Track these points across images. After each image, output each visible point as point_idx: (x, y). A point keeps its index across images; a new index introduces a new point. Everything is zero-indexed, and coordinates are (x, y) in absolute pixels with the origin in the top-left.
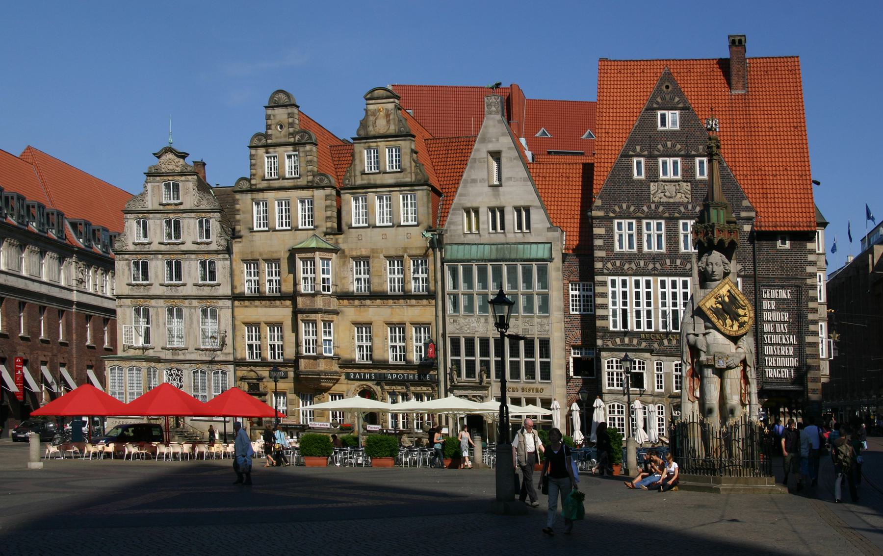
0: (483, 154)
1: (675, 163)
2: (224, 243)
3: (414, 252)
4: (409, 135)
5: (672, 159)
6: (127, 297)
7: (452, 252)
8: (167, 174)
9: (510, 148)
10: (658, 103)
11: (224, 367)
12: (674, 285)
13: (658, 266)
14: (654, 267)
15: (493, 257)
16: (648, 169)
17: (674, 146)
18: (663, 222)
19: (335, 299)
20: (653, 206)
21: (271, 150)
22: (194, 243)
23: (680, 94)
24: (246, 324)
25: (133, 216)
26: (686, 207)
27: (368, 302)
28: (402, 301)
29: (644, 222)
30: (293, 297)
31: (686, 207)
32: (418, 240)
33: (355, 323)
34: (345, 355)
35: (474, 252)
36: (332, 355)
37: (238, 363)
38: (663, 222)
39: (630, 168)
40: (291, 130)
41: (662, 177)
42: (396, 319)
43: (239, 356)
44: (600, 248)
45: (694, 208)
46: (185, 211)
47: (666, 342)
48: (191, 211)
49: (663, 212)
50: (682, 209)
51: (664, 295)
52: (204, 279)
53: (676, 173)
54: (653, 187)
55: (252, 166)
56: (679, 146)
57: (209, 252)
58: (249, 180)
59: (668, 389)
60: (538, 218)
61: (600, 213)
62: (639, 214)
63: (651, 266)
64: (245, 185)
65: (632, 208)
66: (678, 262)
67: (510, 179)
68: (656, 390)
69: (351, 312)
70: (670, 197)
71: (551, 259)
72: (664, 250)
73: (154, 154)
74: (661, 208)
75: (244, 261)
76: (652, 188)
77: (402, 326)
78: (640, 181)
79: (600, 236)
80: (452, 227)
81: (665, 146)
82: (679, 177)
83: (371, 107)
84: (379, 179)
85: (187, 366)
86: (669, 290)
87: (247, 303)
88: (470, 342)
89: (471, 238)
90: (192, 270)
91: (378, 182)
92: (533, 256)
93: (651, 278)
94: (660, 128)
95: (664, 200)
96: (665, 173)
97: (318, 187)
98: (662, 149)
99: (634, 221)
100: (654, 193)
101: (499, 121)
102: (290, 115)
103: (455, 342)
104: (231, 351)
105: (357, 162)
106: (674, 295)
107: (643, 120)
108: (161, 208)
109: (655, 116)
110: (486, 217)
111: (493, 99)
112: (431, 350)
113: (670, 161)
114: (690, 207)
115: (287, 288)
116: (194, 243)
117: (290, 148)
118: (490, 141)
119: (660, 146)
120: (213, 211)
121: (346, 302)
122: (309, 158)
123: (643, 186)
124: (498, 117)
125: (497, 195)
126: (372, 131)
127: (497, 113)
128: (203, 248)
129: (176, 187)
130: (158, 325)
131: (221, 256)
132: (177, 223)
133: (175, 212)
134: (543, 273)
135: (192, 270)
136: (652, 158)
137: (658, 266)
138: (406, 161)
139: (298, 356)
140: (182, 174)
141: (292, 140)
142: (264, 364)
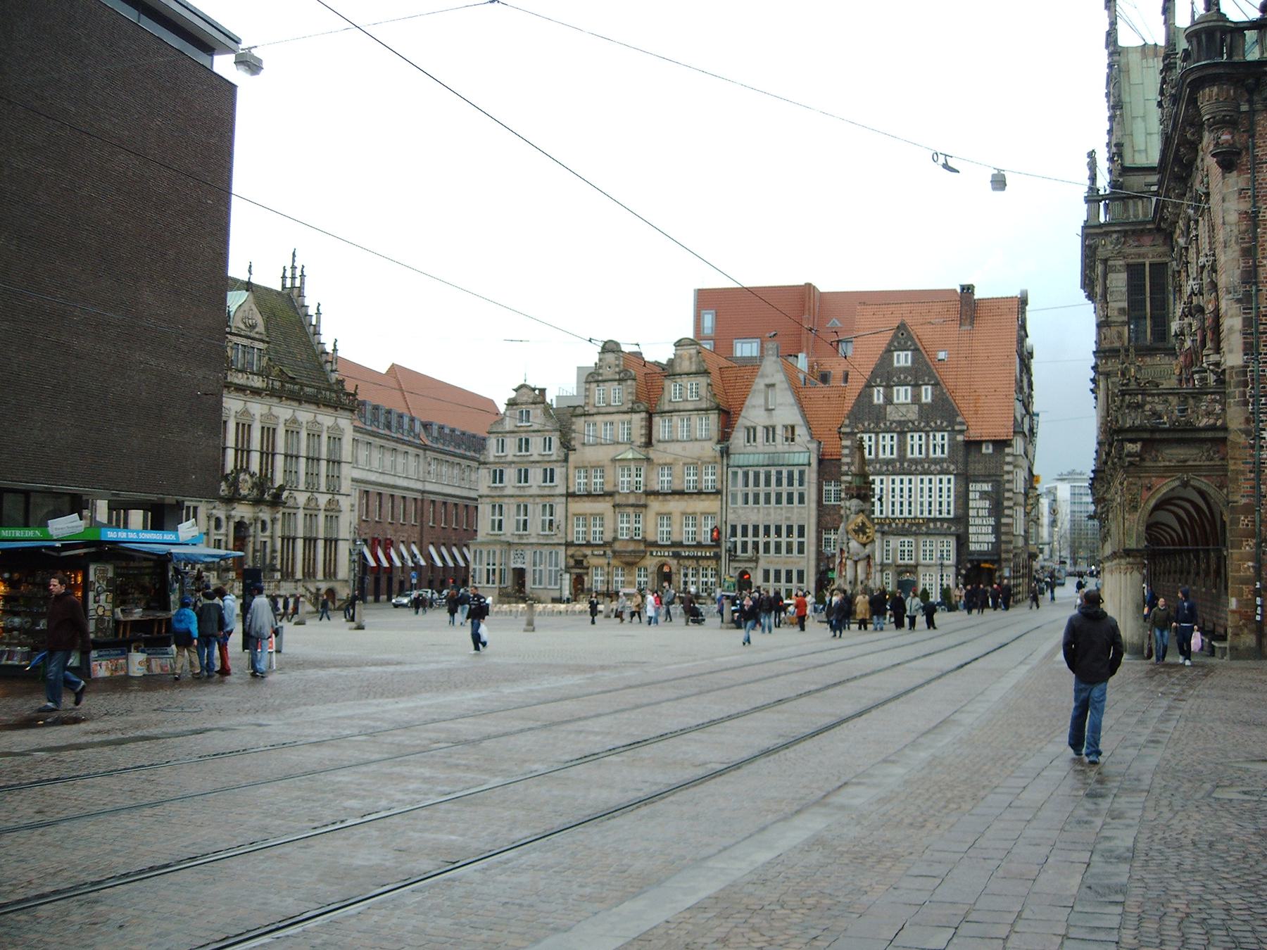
0: (762, 386)
1: (906, 390)
2: (562, 455)
3: (706, 459)
4: (706, 373)
5: (904, 388)
6: (487, 496)
7: (735, 460)
8: (522, 404)
9: (782, 382)
11: (557, 548)
13: (890, 468)
15: (766, 463)
16: (885, 397)
17: (906, 378)
19: (644, 496)
20: (888, 424)
21: (601, 384)
22: (540, 455)
23: (912, 339)
24: (575, 515)
25: (496, 435)
26: (913, 423)
27: (669, 497)
28: (695, 496)
29: (881, 436)
30: (611, 494)
31: (913, 423)
32: (710, 449)
33: (658, 514)
34: (651, 538)
35: (752, 460)
36: (640, 538)
37: (568, 545)
39: (871, 396)
40: (617, 369)
41: (895, 401)
42: (689, 510)
43: (569, 540)
44: (846, 456)
45: (919, 423)
46: (534, 431)
47: (894, 525)
48: (539, 431)
51: (893, 490)
52: (545, 481)
53: (906, 398)
54: (889, 409)
55: (586, 397)
56: (909, 378)
57: (549, 462)
58: (583, 407)
59: (894, 560)
60: (801, 431)
61: (848, 430)
62: (877, 430)
63: (884, 468)
64: (579, 411)
65: (872, 425)
66: (906, 465)
67: (781, 405)
68: (885, 561)
69: (656, 505)
71: (809, 464)
72: (895, 456)
73: (516, 390)
75: (576, 468)
77: (694, 515)
78: (879, 405)
79: (846, 447)
80: (736, 441)
81: (899, 378)
83: (678, 352)
84: (682, 406)
85: (529, 547)
86: (897, 486)
87: (577, 499)
88: (745, 528)
89: (750, 449)
90: (536, 475)
91: (681, 408)
92: (796, 462)
93: (884, 478)
95: (897, 418)
96: (898, 398)
97: (636, 412)
99: (873, 436)
101: (775, 362)
102: (617, 359)
103: (734, 528)
104: (561, 535)
105: (666, 393)
106: (902, 490)
107: (882, 358)
108: (516, 429)
109: (892, 356)
110: (760, 433)
111: (770, 346)
112: (715, 534)
113: (902, 389)
115: (608, 488)
116: (540, 455)
117: (616, 383)
118: (767, 376)
119: (895, 379)
120: (556, 430)
121: (652, 497)
122: (630, 390)
123: (881, 408)
124: (774, 358)
125: (770, 417)
126: (678, 370)
127: (772, 355)
128: (546, 459)
129: (528, 412)
130: (509, 517)
131: (559, 464)
132: (527, 441)
133: (526, 432)
134: (801, 473)
135: (536, 475)
136: (889, 387)
137: (890, 468)
138: (703, 392)
139: (615, 539)
140: (534, 403)
141: (617, 377)
142: (588, 545)
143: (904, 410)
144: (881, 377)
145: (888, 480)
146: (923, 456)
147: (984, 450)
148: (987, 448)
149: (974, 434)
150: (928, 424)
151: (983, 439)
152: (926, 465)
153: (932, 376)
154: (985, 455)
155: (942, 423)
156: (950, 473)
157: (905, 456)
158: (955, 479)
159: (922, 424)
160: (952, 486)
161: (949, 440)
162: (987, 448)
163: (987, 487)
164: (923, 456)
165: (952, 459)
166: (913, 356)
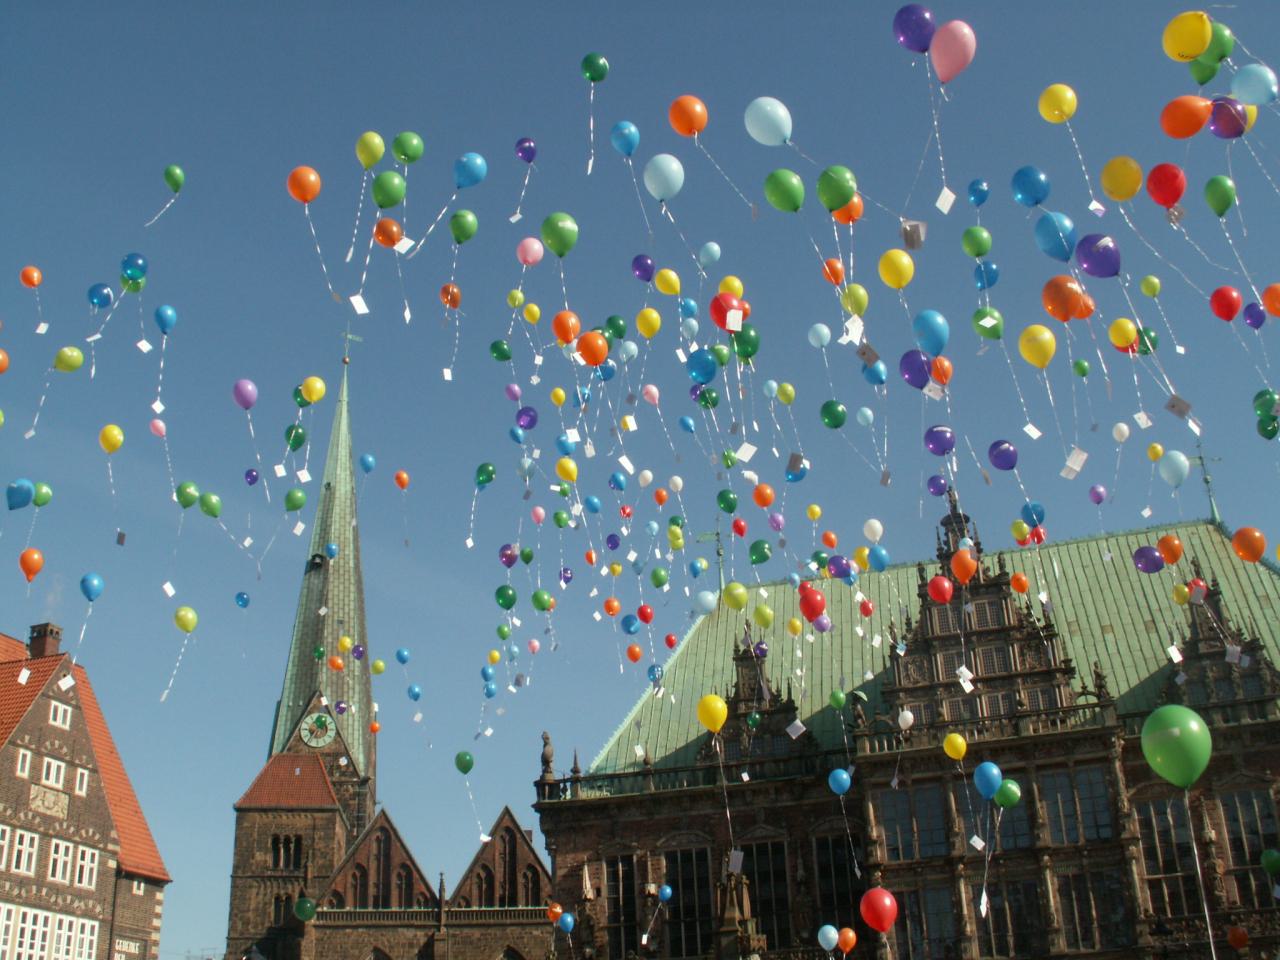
10: (53, 692)
12: (35, 918)
14: (20, 894)
17: (61, 747)
18: (36, 836)
26: (61, 825)
31: (61, 825)
38: (36, 836)
39: (14, 760)
41: (44, 781)
45: (68, 828)
49: (39, 825)
50: (57, 825)
54: (34, 789)
56: (65, 750)
62: (15, 822)
63: (16, 892)
65: (9, 812)
66: (44, 891)
70: (48, 808)
72: (32, 874)
74: (37, 820)
76: (32, 792)
78: (23, 780)
81: (52, 744)
82: (60, 786)
86: (29, 926)
94: (51, 722)
95: (42, 810)
96: (47, 778)
98: (49, 747)
100: (34, 799)
106: (33, 933)
109: (49, 705)
113: (55, 763)
114: (65, 825)
119: (48, 743)
123: (24, 786)
136: (38, 754)
143: (51, 797)
144: (31, 733)
145: (18, 912)
146: (67, 882)
147: (135, 891)
148: (139, 888)
149: (129, 867)
150: (77, 832)
151: (140, 871)
152: (69, 898)
153: (91, 758)
154: (134, 896)
155: (94, 834)
156: (93, 918)
157: (45, 876)
158: (100, 927)
159: (72, 829)
160: (95, 938)
161: (100, 863)
162: (139, 888)
163: (133, 948)
164: (67, 882)
165: (97, 896)
166: (73, 716)
